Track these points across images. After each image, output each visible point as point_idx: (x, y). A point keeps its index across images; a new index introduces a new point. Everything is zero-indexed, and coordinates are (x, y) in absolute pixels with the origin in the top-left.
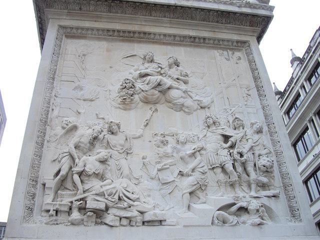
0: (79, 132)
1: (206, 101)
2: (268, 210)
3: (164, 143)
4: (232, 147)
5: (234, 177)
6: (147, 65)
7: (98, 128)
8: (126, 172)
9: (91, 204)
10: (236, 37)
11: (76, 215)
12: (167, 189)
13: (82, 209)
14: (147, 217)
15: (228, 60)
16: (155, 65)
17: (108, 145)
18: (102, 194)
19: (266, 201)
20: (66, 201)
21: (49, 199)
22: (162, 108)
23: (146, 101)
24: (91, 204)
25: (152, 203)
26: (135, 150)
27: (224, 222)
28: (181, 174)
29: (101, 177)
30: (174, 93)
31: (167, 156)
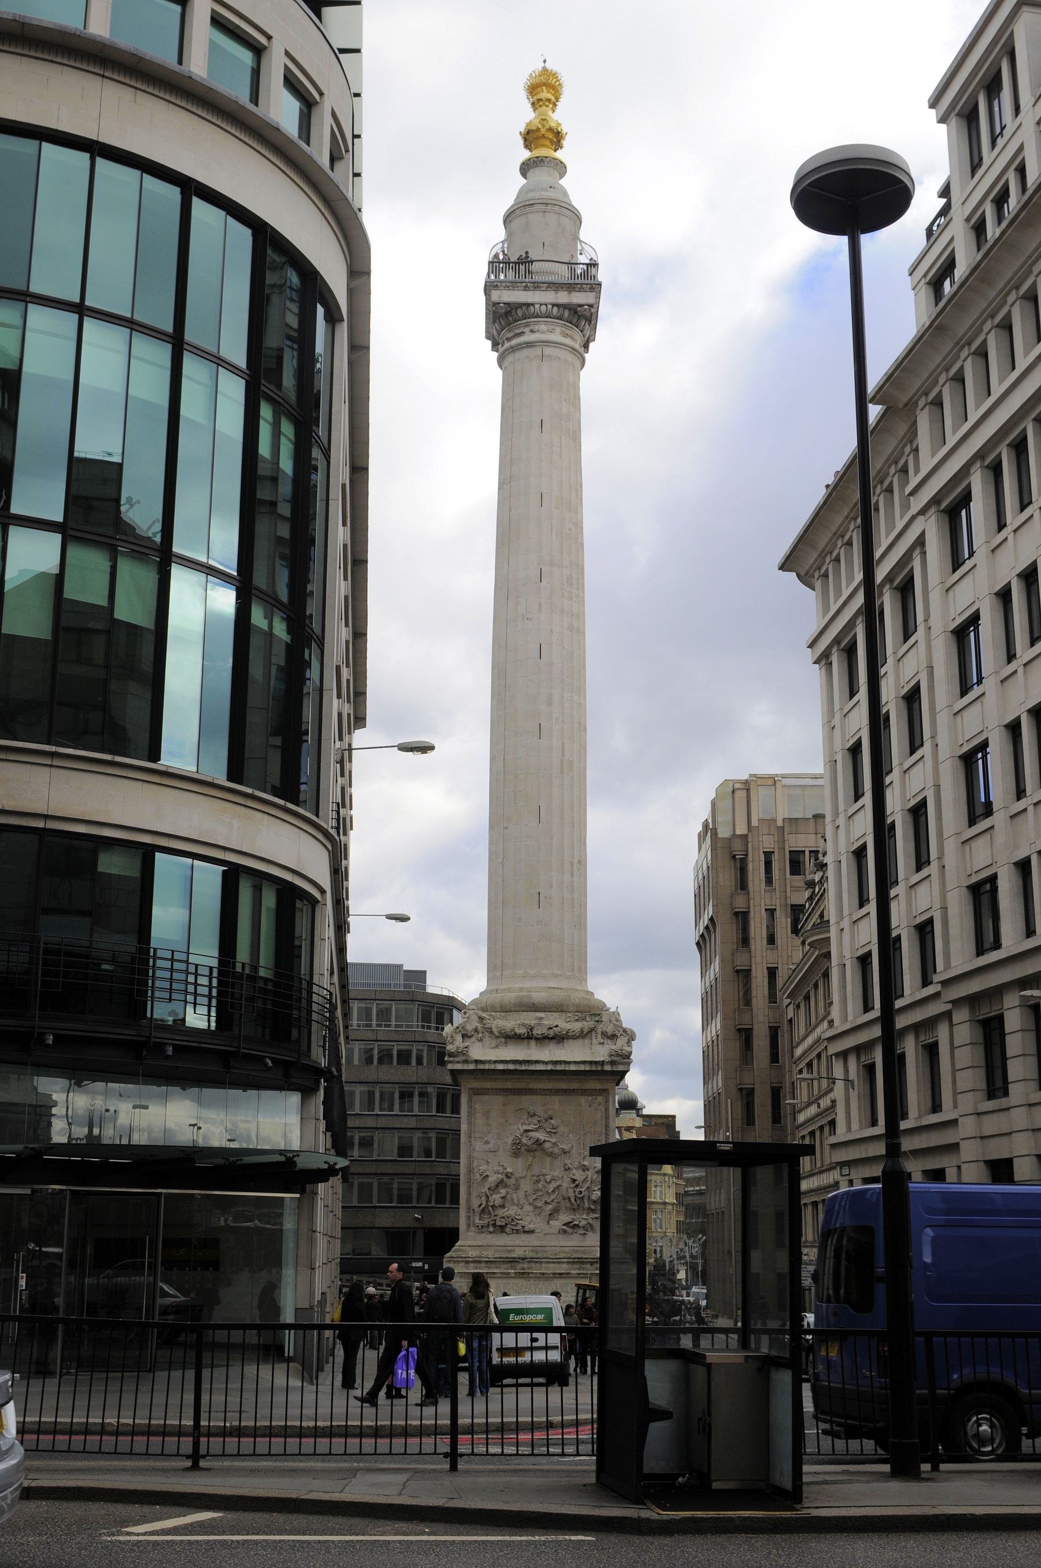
0: (490, 1179)
1: (566, 1147)
2: (591, 1226)
3: (538, 1181)
4: (577, 1186)
5: (575, 1206)
6: (530, 1120)
7: (500, 1176)
8: (516, 1202)
9: (498, 1223)
10: (599, 1086)
11: (491, 1229)
12: (538, 1211)
13: (494, 1225)
14: (526, 1229)
15: (590, 1106)
16: (535, 1120)
17: (506, 1186)
18: (503, 1218)
19: (590, 1221)
20: (486, 1221)
21: (477, 1221)
22: (538, 1154)
23: (529, 1151)
24: (498, 1223)
25: (530, 1221)
26: (522, 1186)
27: (565, 1232)
28: (546, 1203)
29: (503, 1206)
30: (547, 1145)
31: (539, 1190)
